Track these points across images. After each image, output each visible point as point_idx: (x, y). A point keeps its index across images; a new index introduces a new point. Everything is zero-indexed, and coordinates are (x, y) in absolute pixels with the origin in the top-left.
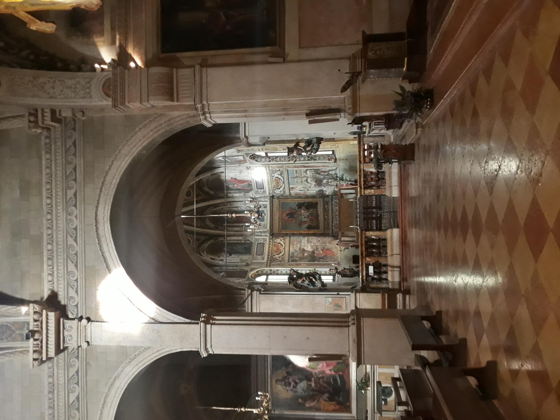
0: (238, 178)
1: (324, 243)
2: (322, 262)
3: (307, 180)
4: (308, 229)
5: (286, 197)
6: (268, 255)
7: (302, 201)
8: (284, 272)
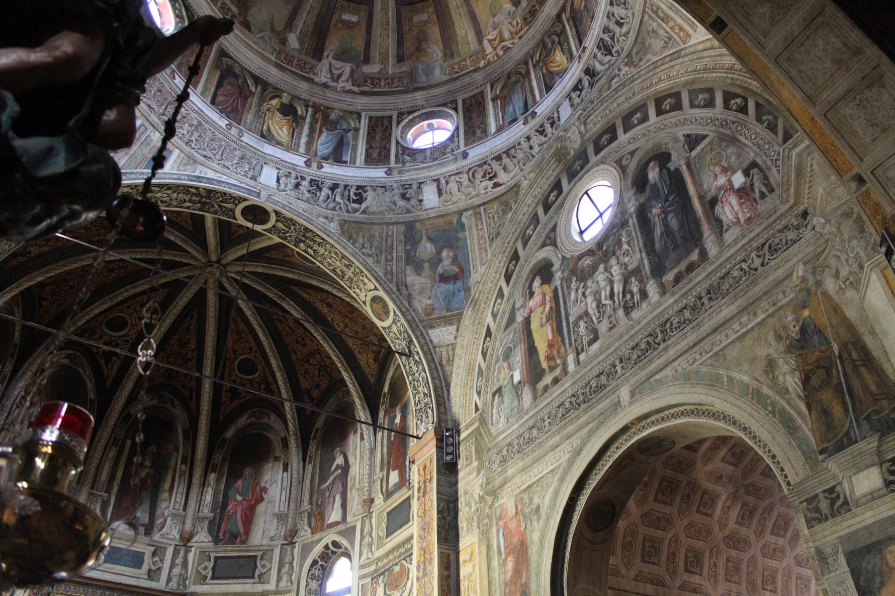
0: (261, 508)
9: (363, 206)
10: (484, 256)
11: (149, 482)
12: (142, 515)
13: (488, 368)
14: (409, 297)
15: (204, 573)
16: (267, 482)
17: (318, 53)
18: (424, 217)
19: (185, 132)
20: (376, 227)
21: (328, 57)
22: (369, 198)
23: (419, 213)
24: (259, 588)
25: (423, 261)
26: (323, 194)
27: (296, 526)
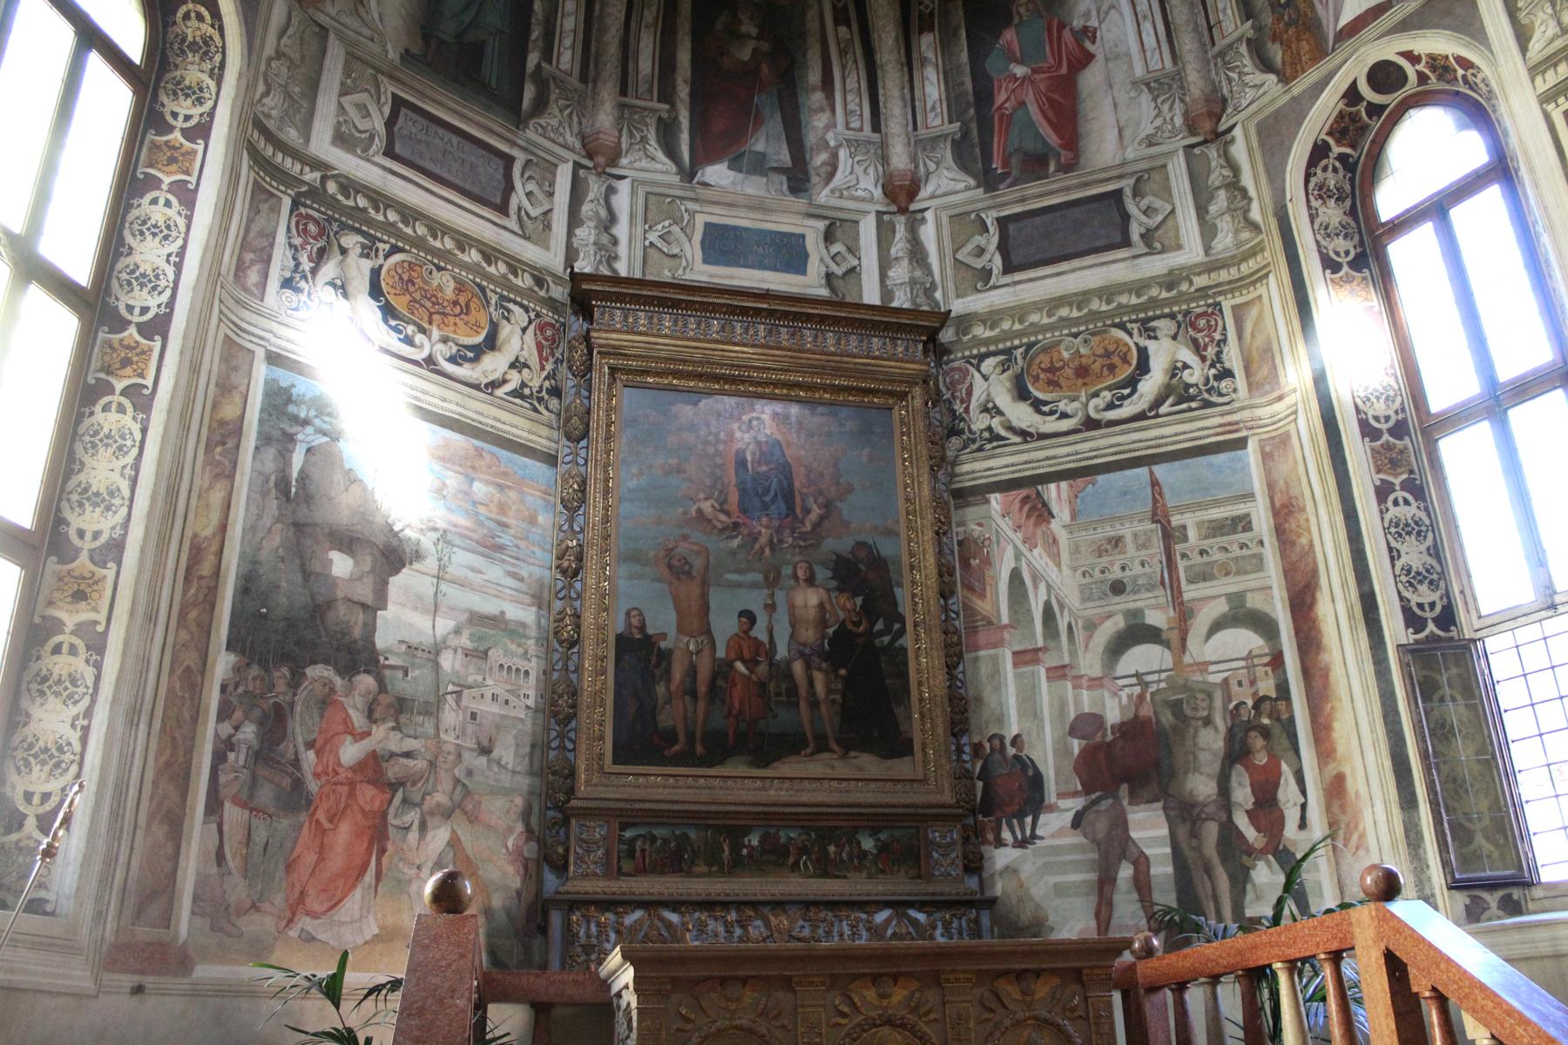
0: (1091, 79)
1: (462, 806)
2: (210, 730)
3: (1152, 635)
4: (624, 644)
5: (941, 463)
6: (379, 199)
7: (915, 594)
8: (149, 254)
11: (765, 69)
12: (768, 142)
15: (978, 263)
16: (1087, 14)
24: (1156, 266)
27: (1215, 89)
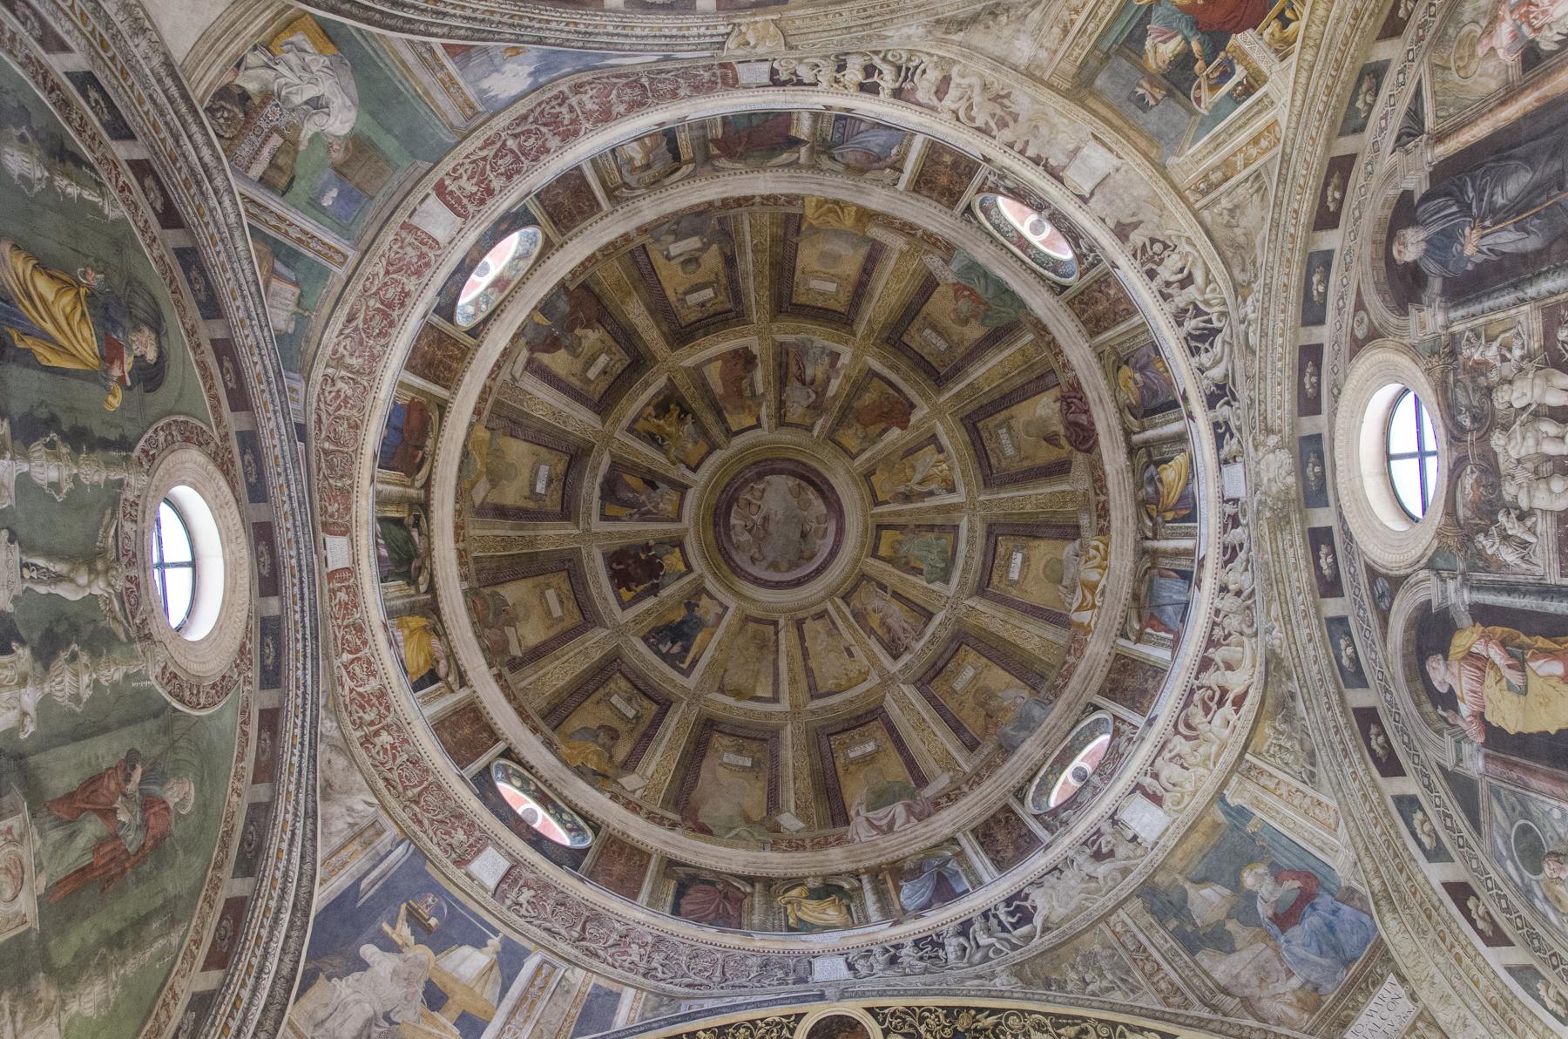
9: (1038, 921)
10: (1322, 816)
13: (1531, 939)
14: (1248, 1004)
17: (840, 816)
18: (1161, 858)
19: (636, 959)
20: (1087, 936)
21: (858, 814)
22: (1038, 903)
23: (1147, 859)
25: (1220, 924)
26: (950, 949)
